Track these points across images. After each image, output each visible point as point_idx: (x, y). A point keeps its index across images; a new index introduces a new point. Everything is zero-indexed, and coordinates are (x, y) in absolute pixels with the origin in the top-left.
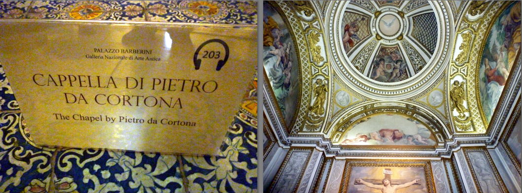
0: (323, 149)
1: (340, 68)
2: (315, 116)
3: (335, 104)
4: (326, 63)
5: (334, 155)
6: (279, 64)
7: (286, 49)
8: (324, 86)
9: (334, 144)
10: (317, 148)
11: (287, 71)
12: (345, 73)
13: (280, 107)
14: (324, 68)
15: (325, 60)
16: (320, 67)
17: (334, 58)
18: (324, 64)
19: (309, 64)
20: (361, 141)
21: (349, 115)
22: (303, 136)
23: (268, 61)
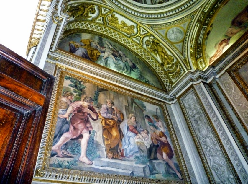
0: (200, 80)
1: (150, 18)
2: (170, 65)
3: (174, 45)
4: (137, 26)
5: (213, 77)
6: (116, 59)
7: (109, 47)
8: (153, 42)
9: (204, 70)
10: (195, 83)
11: (124, 59)
12: (156, 16)
13: (145, 82)
14: (140, 31)
15: (135, 25)
16: (137, 33)
17: (138, 16)
18: (137, 28)
19: (130, 40)
20: (223, 48)
21: (193, 41)
22: (177, 85)
23: (109, 64)
